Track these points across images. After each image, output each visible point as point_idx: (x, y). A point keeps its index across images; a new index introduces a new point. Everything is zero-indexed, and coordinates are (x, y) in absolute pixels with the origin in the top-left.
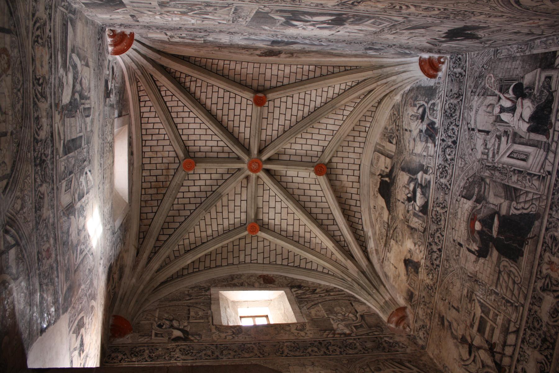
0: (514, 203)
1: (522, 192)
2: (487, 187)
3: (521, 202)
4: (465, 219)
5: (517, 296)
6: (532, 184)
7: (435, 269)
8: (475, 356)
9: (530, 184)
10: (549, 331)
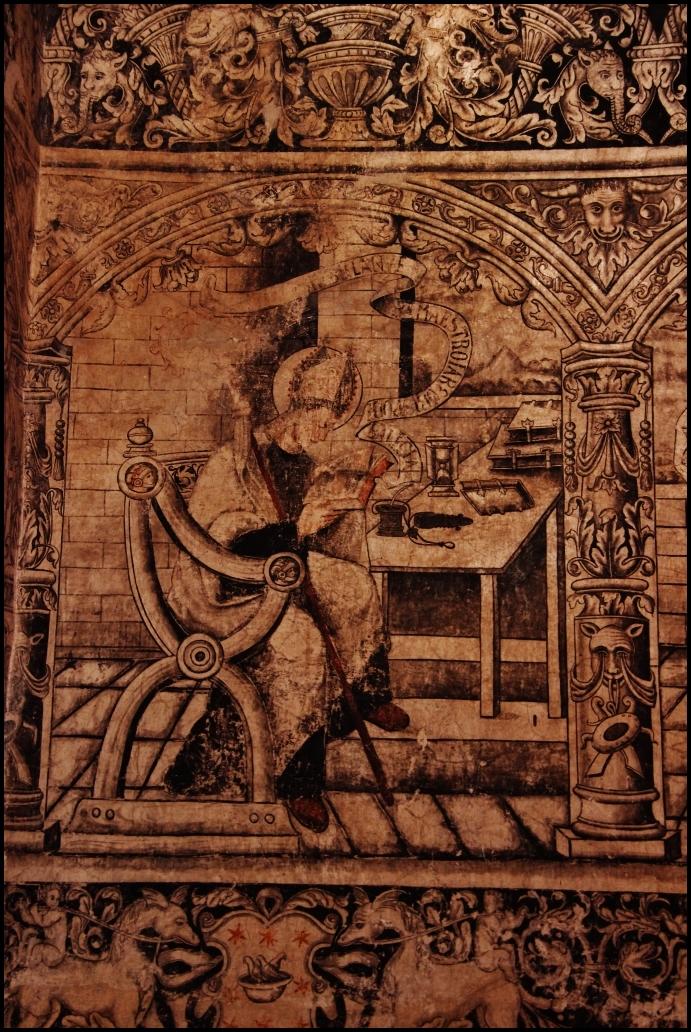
7: (531, 107)
8: (254, 588)
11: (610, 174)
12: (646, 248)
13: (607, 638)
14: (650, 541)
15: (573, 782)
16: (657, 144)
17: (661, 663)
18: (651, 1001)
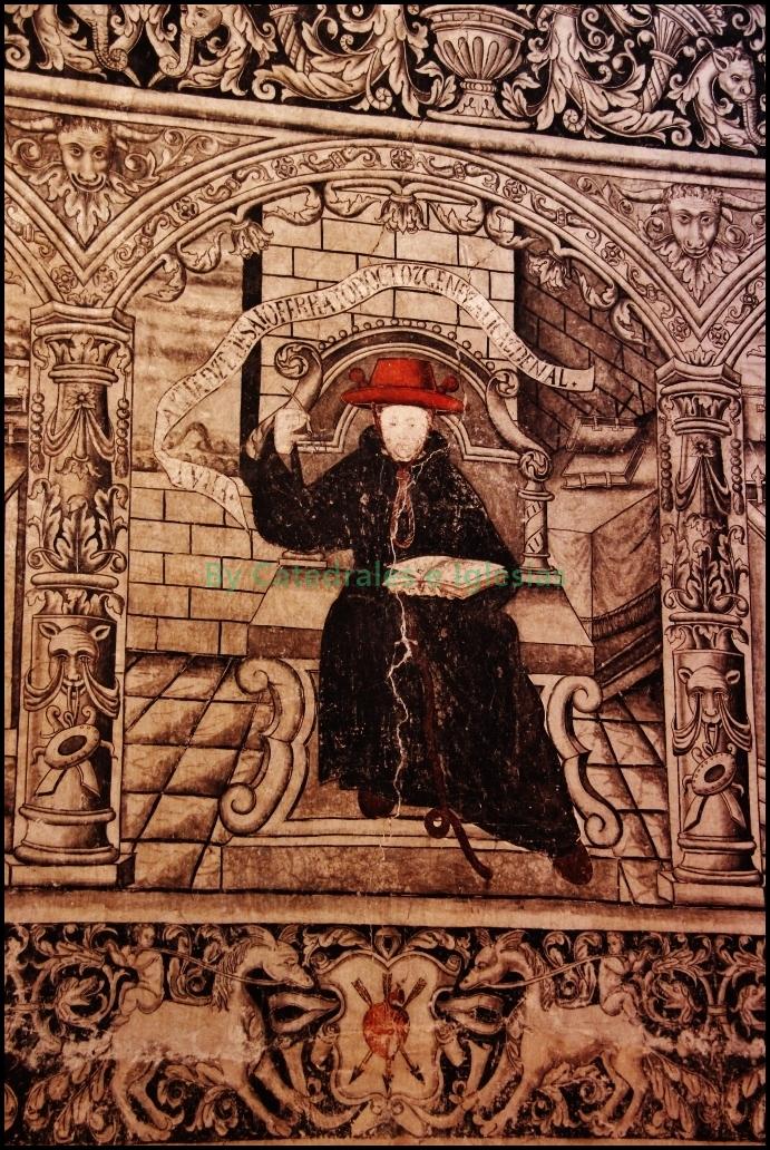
0: (589, 696)
1: (651, 734)
2: (618, 465)
3: (606, 738)
4: (416, 308)
5: (155, 826)
6: (705, 795)
9: (701, 783)
10: (76, 1089)
11: (91, 113)
12: (131, 203)
13: (70, 641)
14: (122, 534)
15: (20, 801)
16: (144, 86)
17: (127, 669)
18: (87, 1040)
